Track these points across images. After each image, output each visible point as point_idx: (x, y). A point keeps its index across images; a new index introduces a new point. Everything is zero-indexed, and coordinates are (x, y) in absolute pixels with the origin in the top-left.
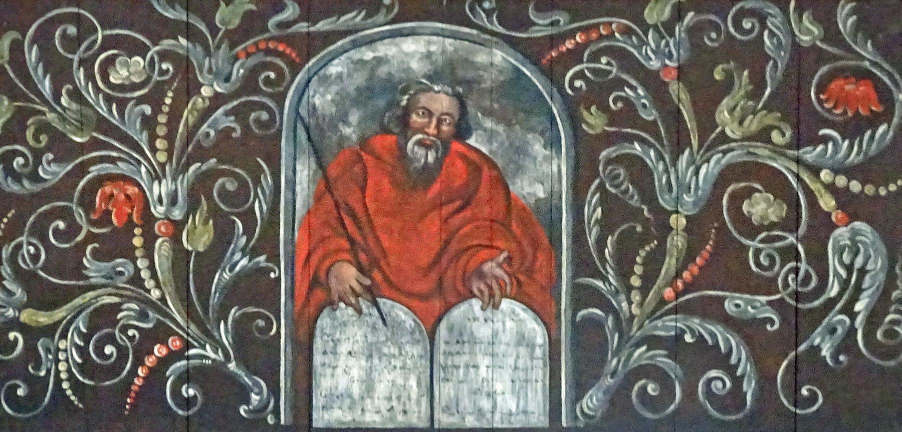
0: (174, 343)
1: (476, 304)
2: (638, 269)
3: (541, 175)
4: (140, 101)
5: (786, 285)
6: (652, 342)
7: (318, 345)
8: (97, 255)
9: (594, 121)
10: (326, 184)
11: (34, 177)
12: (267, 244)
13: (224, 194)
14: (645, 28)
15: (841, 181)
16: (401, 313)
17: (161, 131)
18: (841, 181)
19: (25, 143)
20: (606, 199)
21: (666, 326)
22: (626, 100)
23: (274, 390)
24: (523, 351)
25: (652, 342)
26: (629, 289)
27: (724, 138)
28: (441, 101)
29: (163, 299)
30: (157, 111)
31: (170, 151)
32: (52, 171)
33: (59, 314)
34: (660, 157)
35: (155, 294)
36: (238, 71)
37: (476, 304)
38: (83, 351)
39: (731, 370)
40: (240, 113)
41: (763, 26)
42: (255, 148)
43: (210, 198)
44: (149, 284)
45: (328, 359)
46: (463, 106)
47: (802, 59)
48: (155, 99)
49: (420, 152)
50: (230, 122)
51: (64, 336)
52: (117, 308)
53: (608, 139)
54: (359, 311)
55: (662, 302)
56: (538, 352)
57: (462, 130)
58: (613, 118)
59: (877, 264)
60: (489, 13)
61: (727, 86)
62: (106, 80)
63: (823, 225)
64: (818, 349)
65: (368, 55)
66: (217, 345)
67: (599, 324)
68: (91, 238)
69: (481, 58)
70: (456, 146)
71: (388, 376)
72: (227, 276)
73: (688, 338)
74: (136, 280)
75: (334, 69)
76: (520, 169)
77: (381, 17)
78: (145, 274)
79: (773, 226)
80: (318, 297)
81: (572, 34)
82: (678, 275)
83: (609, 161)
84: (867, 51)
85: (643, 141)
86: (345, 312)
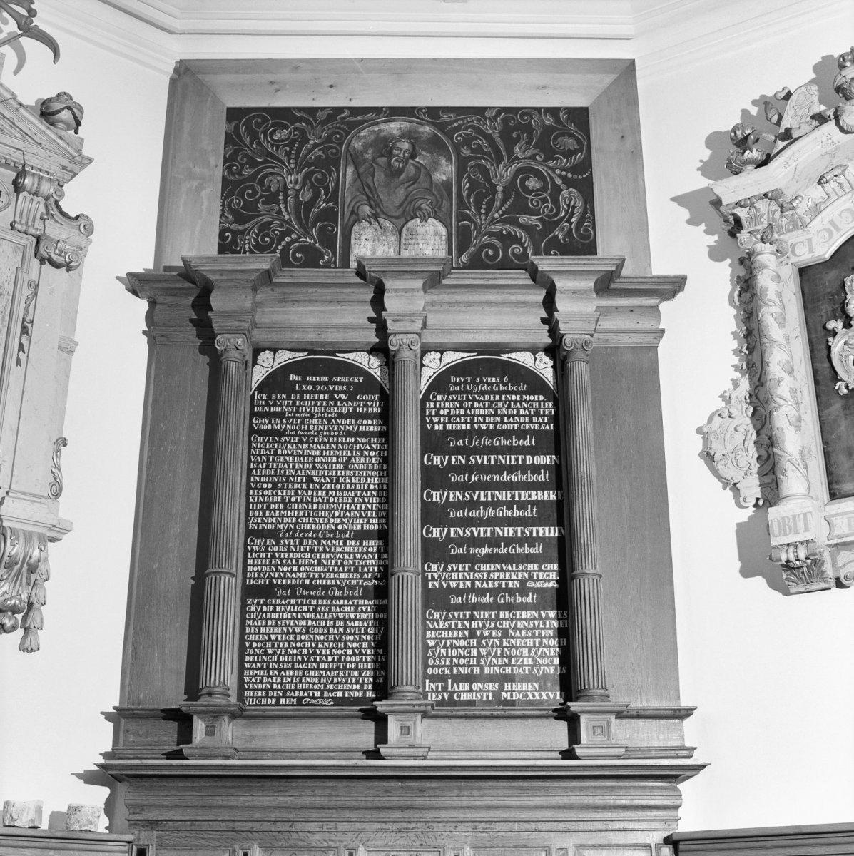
0: (294, 236)
1: (418, 220)
2: (484, 206)
3: (445, 171)
4: (285, 145)
5: (544, 212)
6: (491, 234)
7: (353, 236)
8: (264, 203)
9: (465, 152)
10: (358, 176)
11: (240, 174)
12: (334, 198)
13: (317, 179)
14: (486, 119)
15: (564, 173)
16: (387, 224)
17: (293, 157)
18: (564, 173)
19: (238, 161)
20: (470, 181)
21: (496, 228)
22: (478, 144)
23: (334, 254)
24: (437, 238)
25: (491, 234)
26: (480, 214)
27: (517, 158)
28: (405, 145)
29: (290, 219)
30: (291, 149)
31: (296, 164)
32: (247, 172)
33: (247, 226)
34: (492, 165)
35: (287, 217)
36: (325, 135)
37: (418, 220)
38: (256, 240)
39: (522, 245)
41: (532, 118)
42: (331, 163)
43: (311, 181)
44: (285, 213)
45: (357, 242)
46: (414, 148)
47: (548, 131)
48: (291, 145)
49: (397, 163)
50: (320, 153)
51: (248, 234)
52: (271, 223)
53: (471, 158)
54: (371, 223)
55: (493, 219)
56: (444, 238)
57: (413, 156)
58: (473, 151)
59: (579, 204)
60: (424, 113)
61: (518, 140)
62: (271, 137)
63: (557, 190)
64: (557, 236)
65: (377, 129)
66: (312, 237)
67: (467, 227)
68: (262, 196)
69: (421, 129)
70: (411, 161)
71: (381, 248)
72: (317, 210)
73: (504, 232)
74: (279, 212)
75: (362, 134)
76: (436, 169)
77: (382, 115)
78: (283, 210)
79: (538, 190)
81: (457, 121)
82: (500, 208)
83: (472, 167)
84: (572, 127)
85: (485, 159)
86: (364, 224)
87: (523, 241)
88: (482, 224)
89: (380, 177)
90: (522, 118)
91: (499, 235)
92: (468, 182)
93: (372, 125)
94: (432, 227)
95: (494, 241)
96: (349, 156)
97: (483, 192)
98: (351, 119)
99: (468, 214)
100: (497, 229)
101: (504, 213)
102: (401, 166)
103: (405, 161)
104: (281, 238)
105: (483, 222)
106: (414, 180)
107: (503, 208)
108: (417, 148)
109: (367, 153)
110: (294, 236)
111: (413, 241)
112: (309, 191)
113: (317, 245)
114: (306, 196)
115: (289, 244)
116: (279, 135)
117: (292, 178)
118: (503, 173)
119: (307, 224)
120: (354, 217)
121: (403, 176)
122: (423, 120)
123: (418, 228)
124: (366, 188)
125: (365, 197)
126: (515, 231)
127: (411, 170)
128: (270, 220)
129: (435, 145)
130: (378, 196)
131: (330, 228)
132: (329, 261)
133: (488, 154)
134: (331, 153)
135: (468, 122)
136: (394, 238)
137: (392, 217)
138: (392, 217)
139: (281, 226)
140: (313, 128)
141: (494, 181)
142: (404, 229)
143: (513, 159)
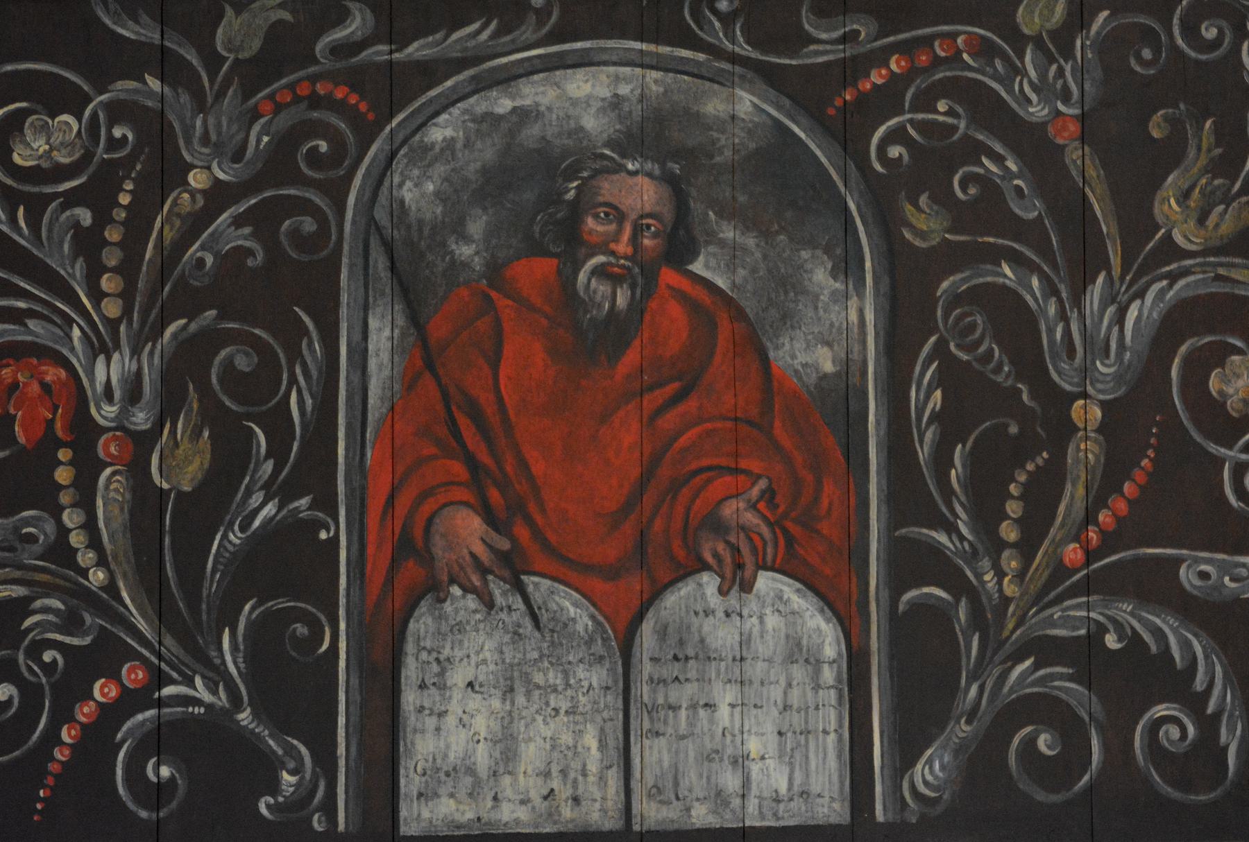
0: (132, 675)
1: (709, 582)
2: (1014, 508)
3: (830, 328)
4: (71, 199)
6: (1045, 650)
7: (411, 671)
9: (925, 223)
10: (423, 356)
12: (311, 473)
14: (1018, 40)
16: (569, 606)
17: (111, 258)
21: (1070, 618)
22: (985, 181)
24: (799, 673)
25: (1045, 650)
27: (1170, 250)
28: (640, 192)
29: (111, 588)
30: (103, 219)
31: (126, 296)
35: (98, 577)
36: (259, 139)
37: (709, 582)
39: (1194, 704)
40: (262, 221)
42: (290, 288)
48: (99, 195)
49: (602, 288)
50: (242, 238)
52: (21, 607)
53: (949, 258)
54: (489, 604)
55: (1060, 571)
56: (828, 675)
57: (680, 244)
58: (961, 216)
60: (727, 20)
61: (1172, 154)
65: (504, 105)
66: (216, 676)
69: (714, 106)
70: (668, 276)
72: (236, 537)
73: (1111, 641)
74: (61, 552)
75: (438, 133)
76: (787, 319)
77: (527, 32)
80: (413, 576)
82: (1090, 518)
83: (956, 299)
85: (1017, 260)
86: (462, 604)
87: (1199, 684)
88: (1006, 601)
89: (527, 359)
90: (1190, 31)
91: (1085, 655)
92: (940, 380)
93: (481, 85)
94: (772, 621)
95: (1066, 686)
96: (374, 242)
97: (1004, 425)
98: (379, 52)
99: (936, 550)
100: (1066, 621)
101: (1111, 542)
102: (622, 300)
103: (641, 276)
104: (71, 687)
105: (1010, 589)
106: (688, 378)
107: (1103, 517)
108: (696, 206)
109: (465, 238)
110: (132, 675)
111: (690, 689)
112: (196, 435)
113: (244, 717)
114: (182, 465)
115: (112, 714)
116: (41, 145)
117: (109, 371)
118: (1114, 325)
119: (193, 599)
120: (411, 570)
121: (631, 358)
122: (714, 51)
123: (708, 625)
124: (463, 421)
125: (458, 469)
126: (1159, 634)
127: (672, 324)
128: (19, 591)
129: (779, 188)
130: (523, 464)
131: (301, 629)
132: (302, 801)
133: (1031, 232)
134: (295, 233)
135: (937, 62)
136: (596, 676)
137: (587, 568)
138: (587, 568)
139: (71, 623)
140: (201, 106)
141: (1063, 377)
142: (647, 627)
143: (1151, 256)
